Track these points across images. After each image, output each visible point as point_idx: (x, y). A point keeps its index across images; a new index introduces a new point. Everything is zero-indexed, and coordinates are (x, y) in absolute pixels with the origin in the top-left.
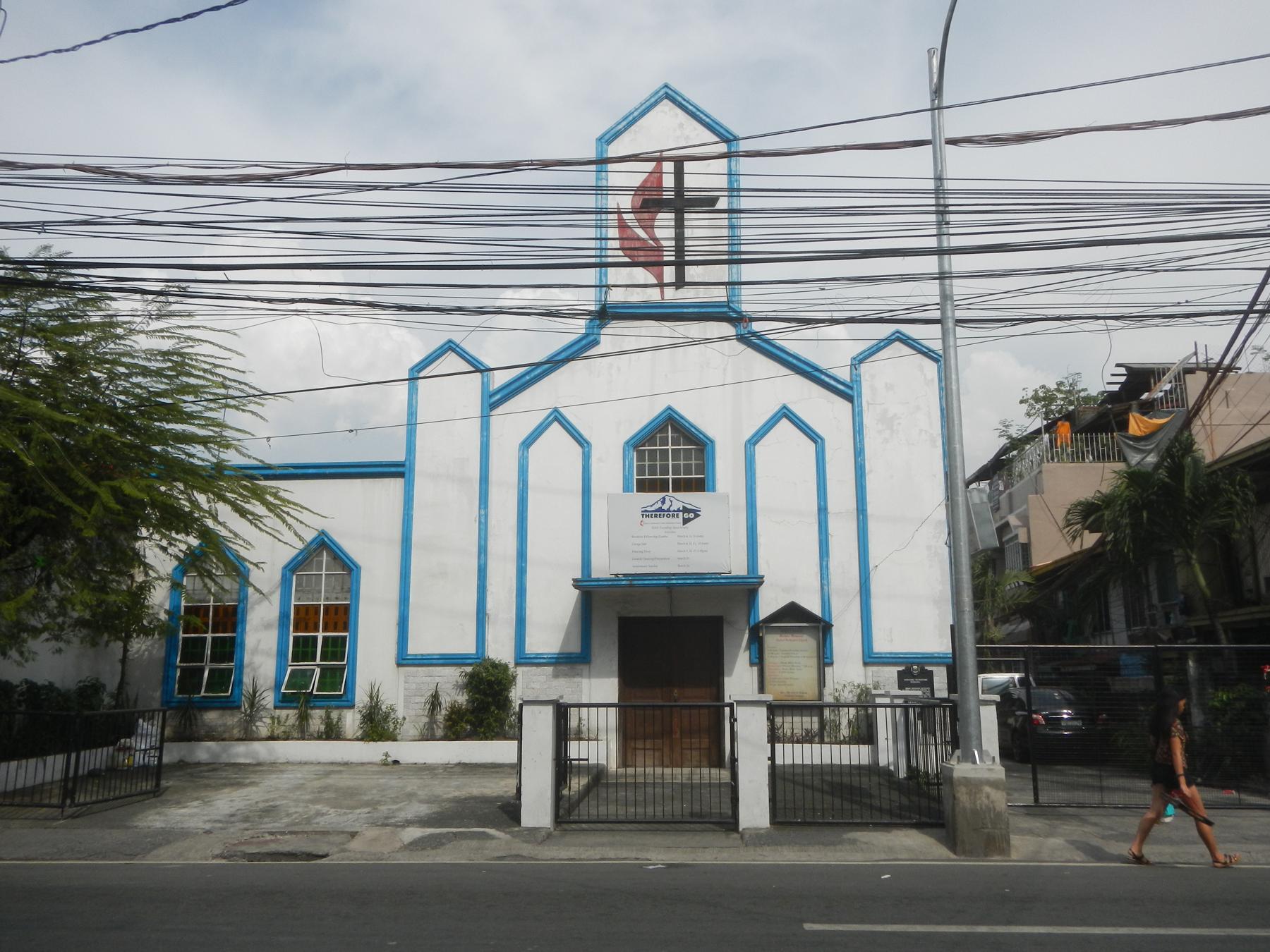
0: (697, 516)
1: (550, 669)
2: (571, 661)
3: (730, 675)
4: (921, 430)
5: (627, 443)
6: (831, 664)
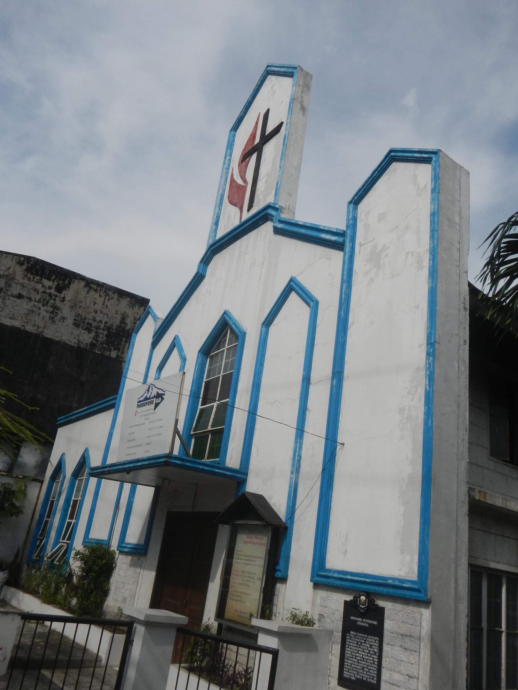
0: (163, 399)
1: (130, 558)
2: (138, 552)
3: (213, 581)
4: (407, 254)
5: (199, 351)
6: (284, 580)
